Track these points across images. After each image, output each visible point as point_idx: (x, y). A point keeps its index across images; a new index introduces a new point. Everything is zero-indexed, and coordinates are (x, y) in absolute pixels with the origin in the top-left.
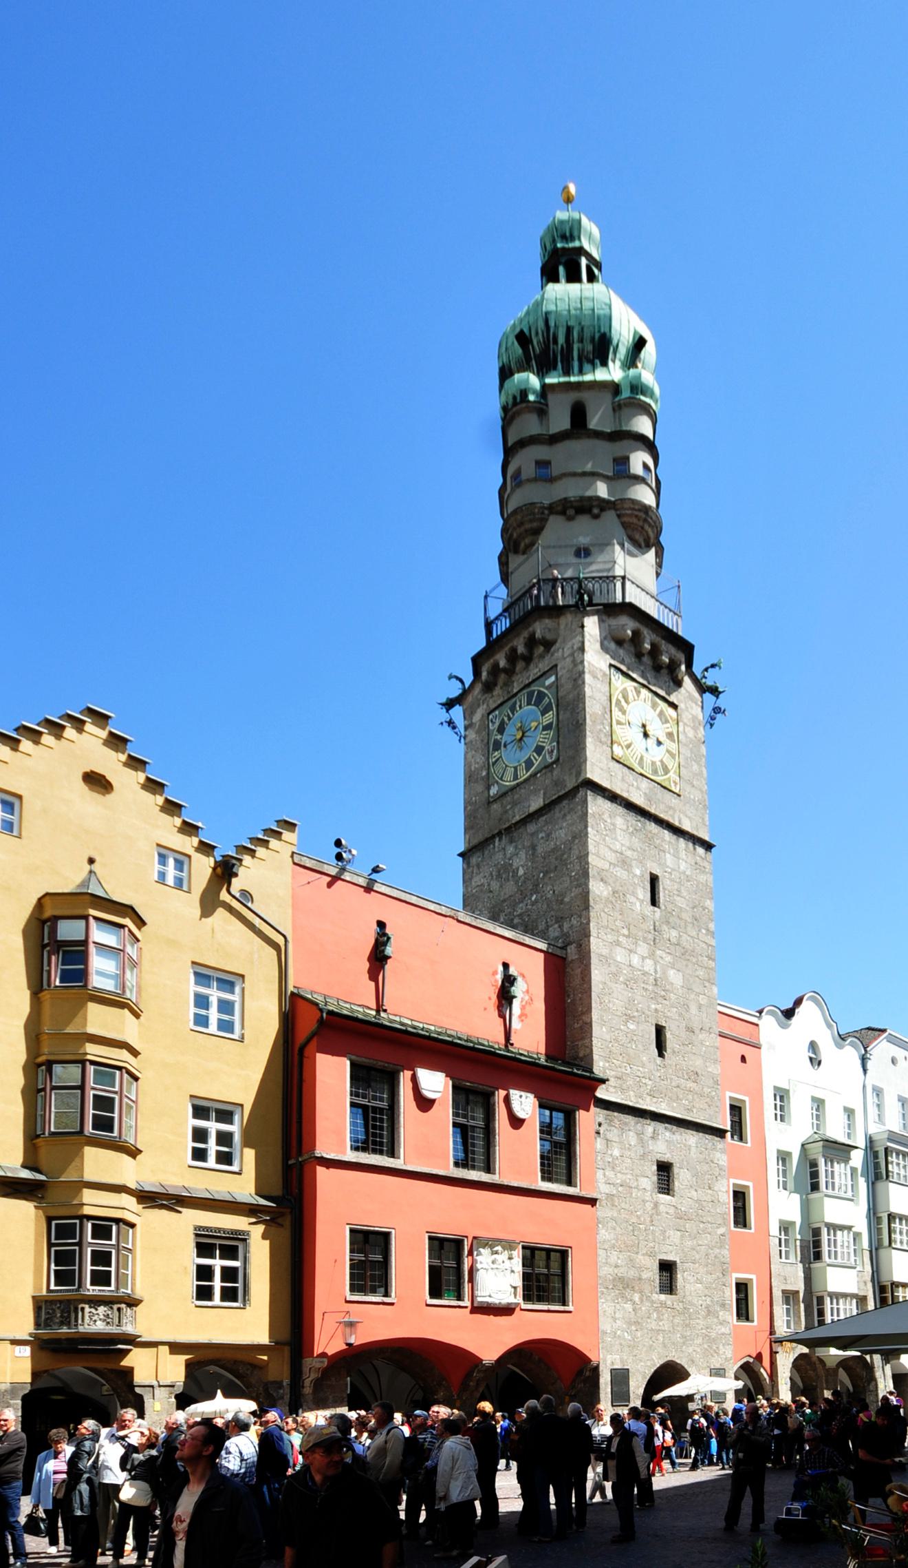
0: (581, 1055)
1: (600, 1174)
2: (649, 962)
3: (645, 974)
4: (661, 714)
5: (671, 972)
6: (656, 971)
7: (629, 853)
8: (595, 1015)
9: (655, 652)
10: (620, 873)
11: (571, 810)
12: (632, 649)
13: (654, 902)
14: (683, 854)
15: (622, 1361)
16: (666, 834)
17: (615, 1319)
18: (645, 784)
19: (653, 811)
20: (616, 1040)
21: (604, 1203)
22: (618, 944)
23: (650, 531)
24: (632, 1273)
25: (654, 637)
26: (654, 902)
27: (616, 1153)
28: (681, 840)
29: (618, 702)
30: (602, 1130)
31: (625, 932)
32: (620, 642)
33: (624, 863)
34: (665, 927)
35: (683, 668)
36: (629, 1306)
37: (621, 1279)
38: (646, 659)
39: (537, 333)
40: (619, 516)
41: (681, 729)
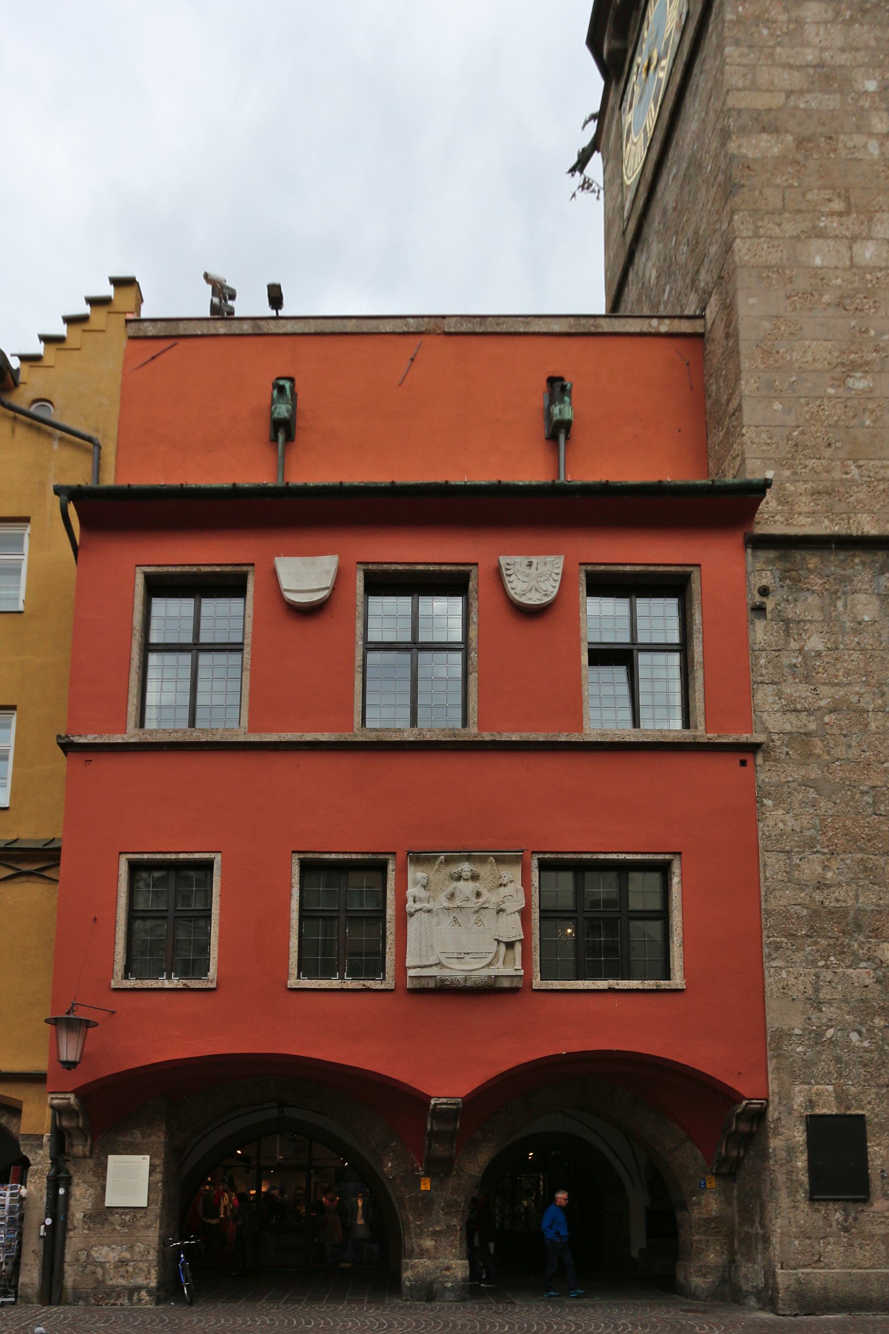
1: (764, 697)
15: (841, 1096)
21: (781, 752)
30: (770, 604)
37: (838, 914)
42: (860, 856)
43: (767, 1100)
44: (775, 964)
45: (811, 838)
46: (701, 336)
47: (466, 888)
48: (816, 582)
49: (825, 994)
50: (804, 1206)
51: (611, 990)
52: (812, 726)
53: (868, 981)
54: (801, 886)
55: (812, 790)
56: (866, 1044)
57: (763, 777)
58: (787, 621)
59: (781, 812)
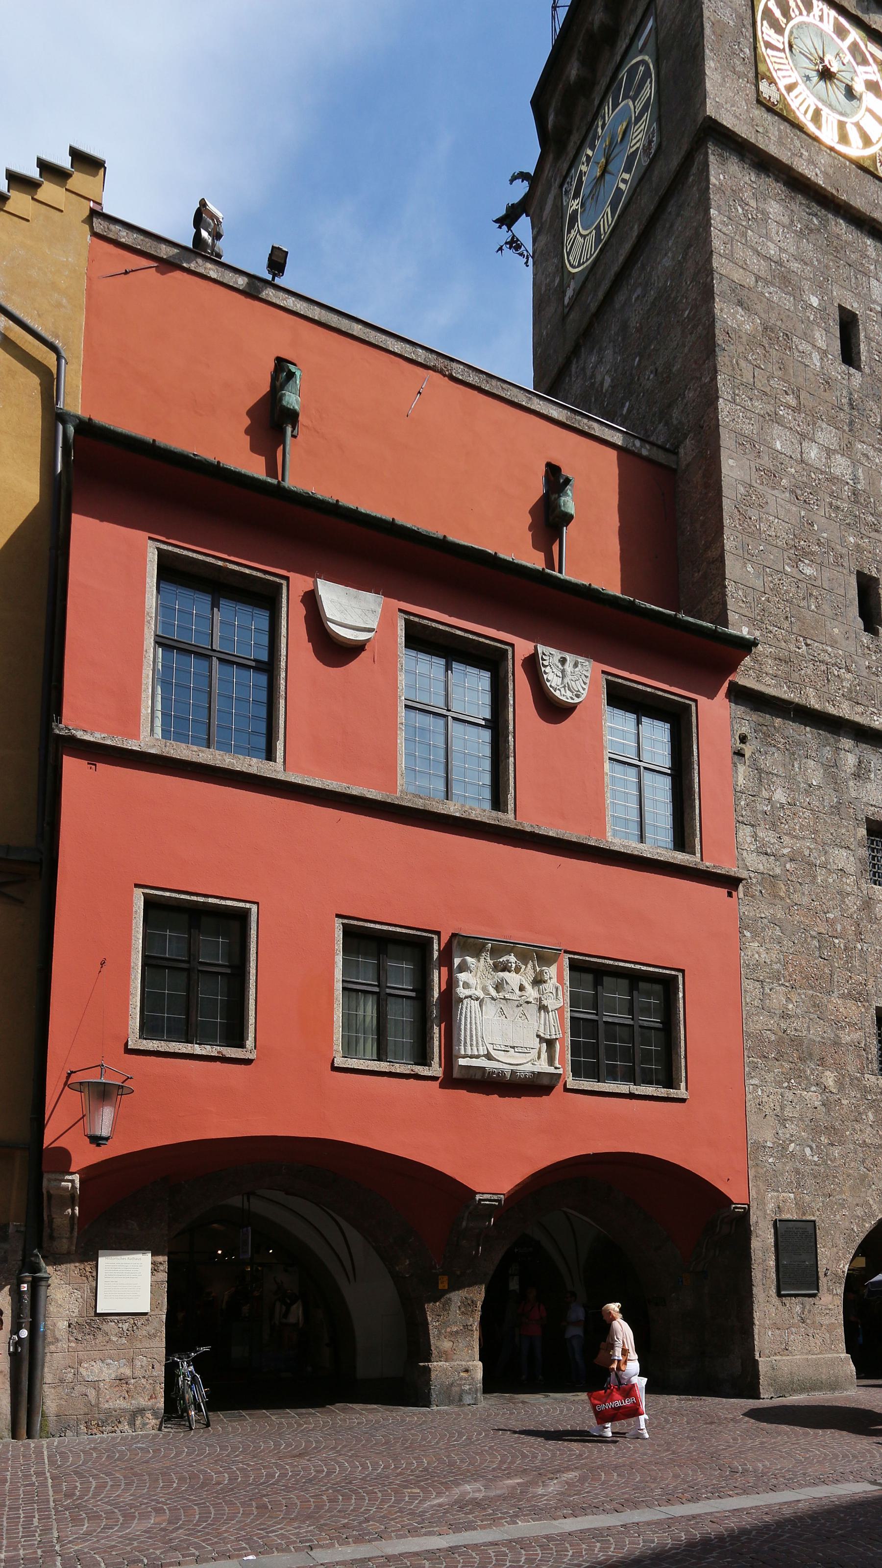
4: (854, 48)
7: (795, 266)
8: (730, 543)
17: (783, 1121)
20: (776, 590)
22: (776, 419)
24: (816, 1032)
29: (767, 12)
30: (748, 750)
31: (791, 400)
33: (785, 280)
36: (813, 1097)
37: (796, 1042)
42: (811, 992)
43: (749, 1205)
44: (753, 1081)
45: (778, 971)
46: (674, 471)
49: (788, 1112)
50: (775, 1299)
52: (778, 871)
53: (817, 1104)
54: (771, 1014)
55: (778, 928)
56: (816, 1158)
59: (756, 944)
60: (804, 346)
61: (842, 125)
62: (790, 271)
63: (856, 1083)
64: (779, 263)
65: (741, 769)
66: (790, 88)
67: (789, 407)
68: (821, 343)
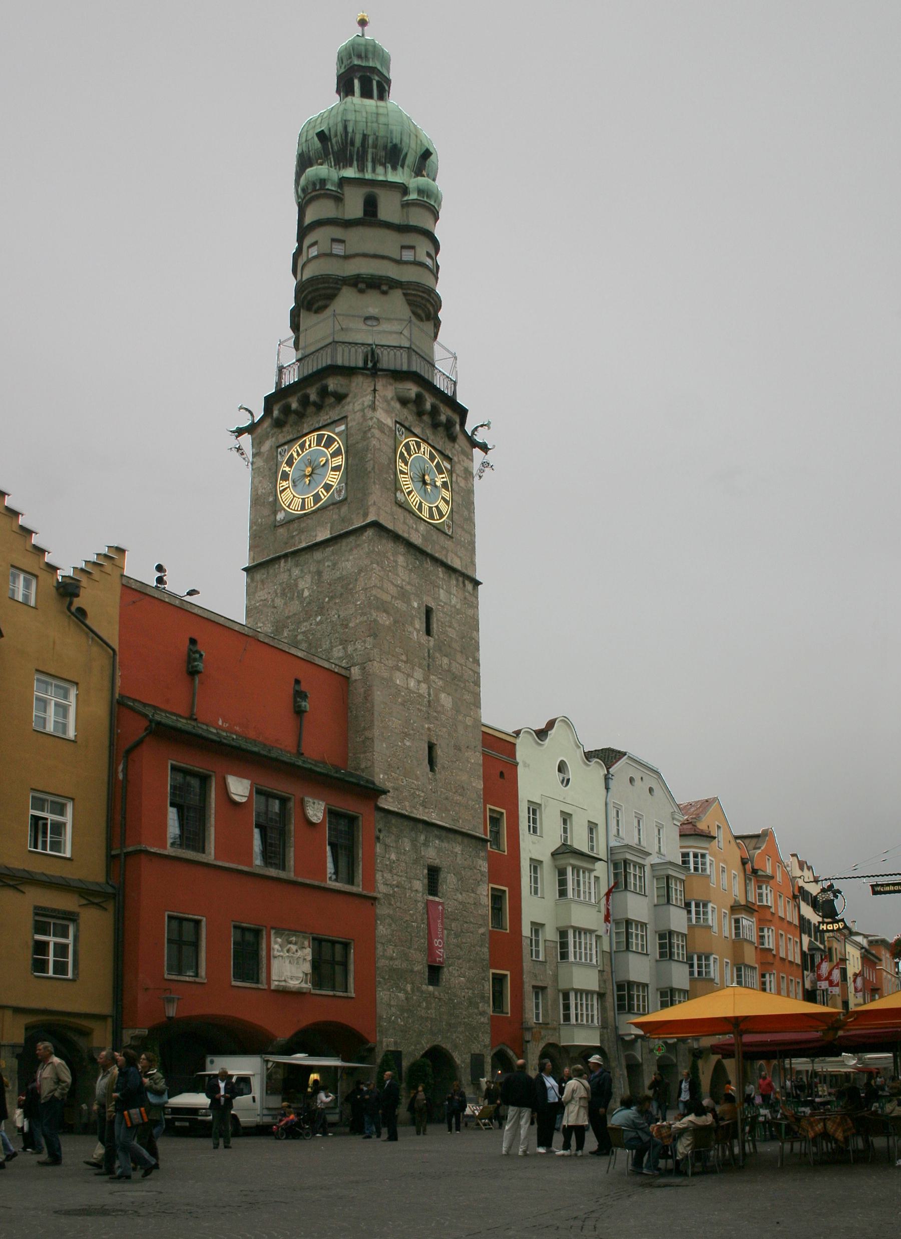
0: (363, 766)
1: (379, 876)
2: (424, 686)
3: (420, 696)
4: (438, 466)
5: (443, 695)
6: (429, 695)
9: (435, 411)
10: (399, 604)
11: (357, 546)
12: (414, 409)
13: (428, 632)
14: (454, 590)
16: (440, 571)
18: (422, 527)
19: (429, 551)
22: (398, 669)
23: (431, 309)
25: (433, 400)
26: (428, 632)
27: (393, 857)
28: (453, 576)
29: (402, 453)
31: (404, 658)
32: (404, 402)
34: (437, 655)
35: (458, 427)
36: (401, 995)
38: (426, 418)
39: (336, 135)
40: (405, 294)
41: (454, 479)
47: (294, 948)
48: (394, 830)
51: (334, 996)
57: (378, 911)
58: (386, 845)
60: (411, 629)
61: (430, 508)
62: (406, 591)
63: (419, 989)
64: (402, 588)
65: (378, 845)
66: (409, 493)
67: (402, 661)
68: (417, 626)
